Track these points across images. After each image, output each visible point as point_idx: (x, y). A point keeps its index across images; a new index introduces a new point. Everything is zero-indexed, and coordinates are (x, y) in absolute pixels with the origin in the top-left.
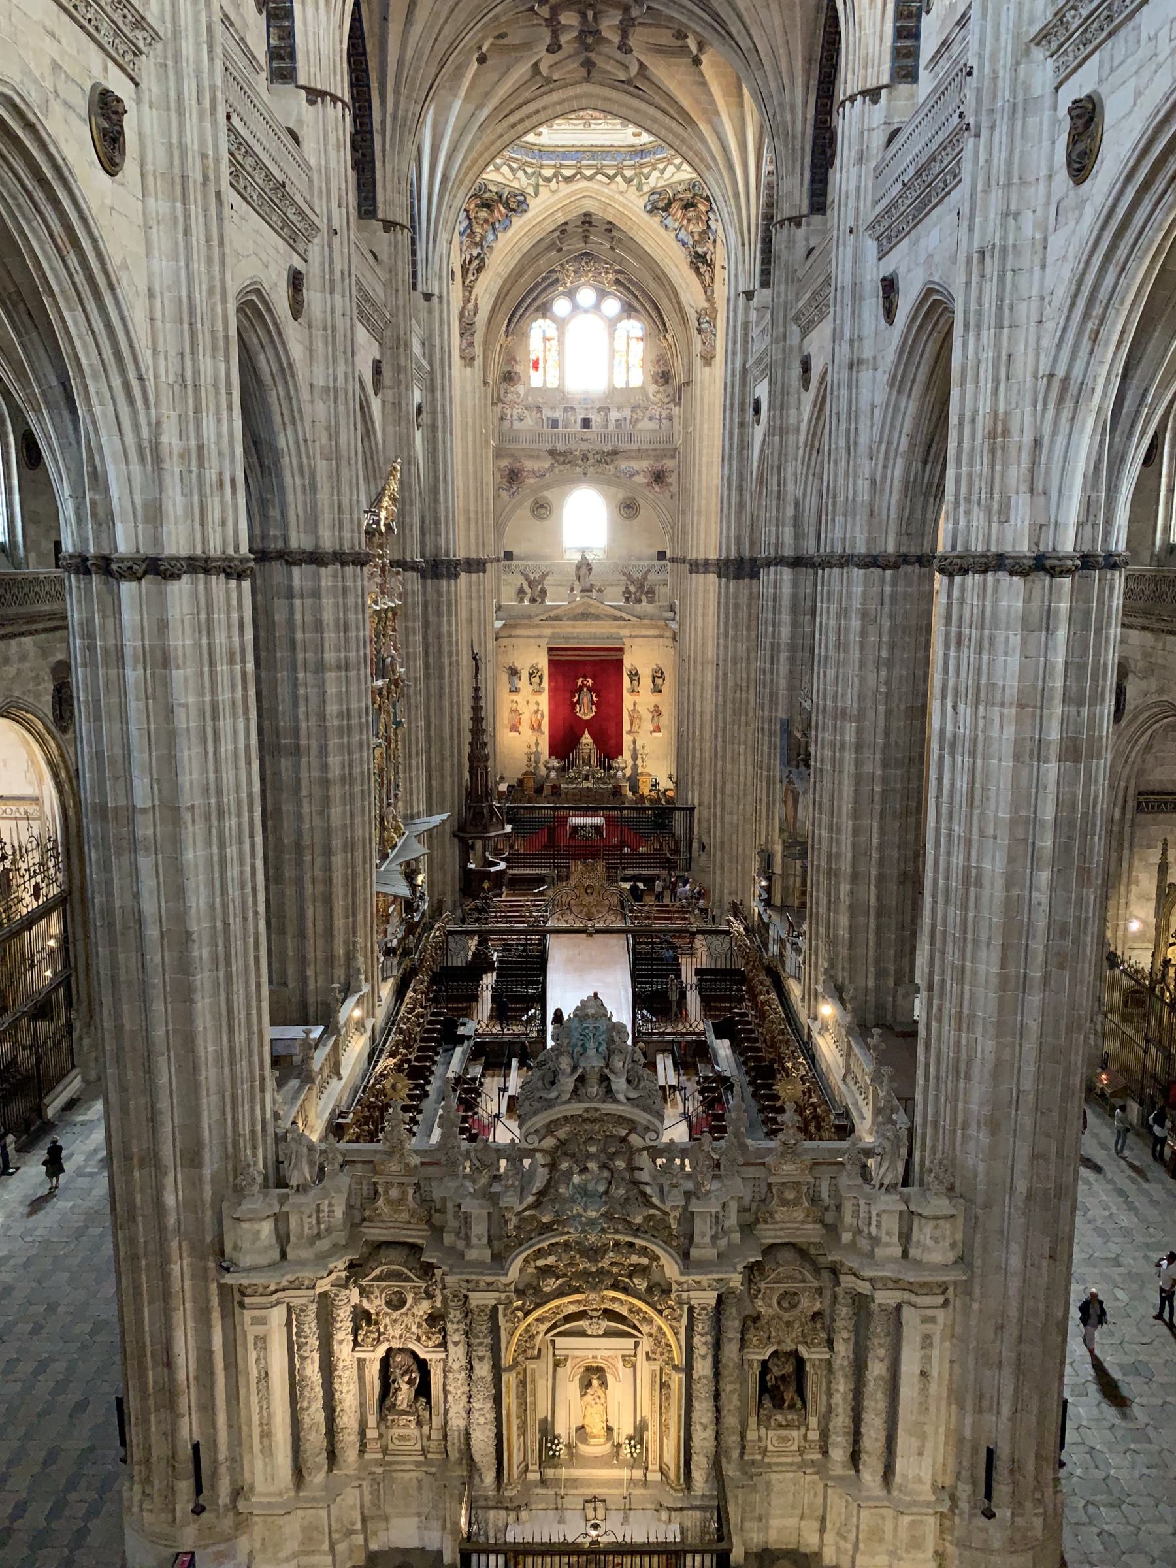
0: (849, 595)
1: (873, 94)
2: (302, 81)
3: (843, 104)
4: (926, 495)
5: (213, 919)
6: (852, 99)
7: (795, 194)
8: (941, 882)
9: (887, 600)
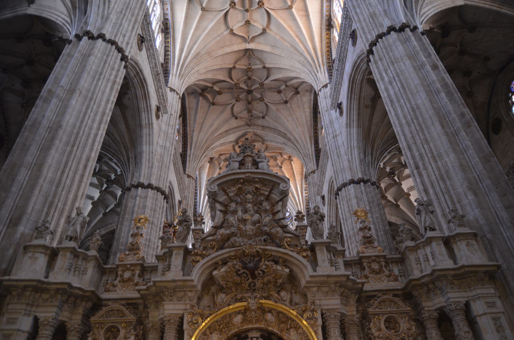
0: (349, 194)
1: (326, 86)
2: (169, 85)
3: (318, 94)
4: (368, 166)
5: (74, 128)
6: (320, 90)
7: (312, 166)
8: (404, 121)
9: (363, 191)
